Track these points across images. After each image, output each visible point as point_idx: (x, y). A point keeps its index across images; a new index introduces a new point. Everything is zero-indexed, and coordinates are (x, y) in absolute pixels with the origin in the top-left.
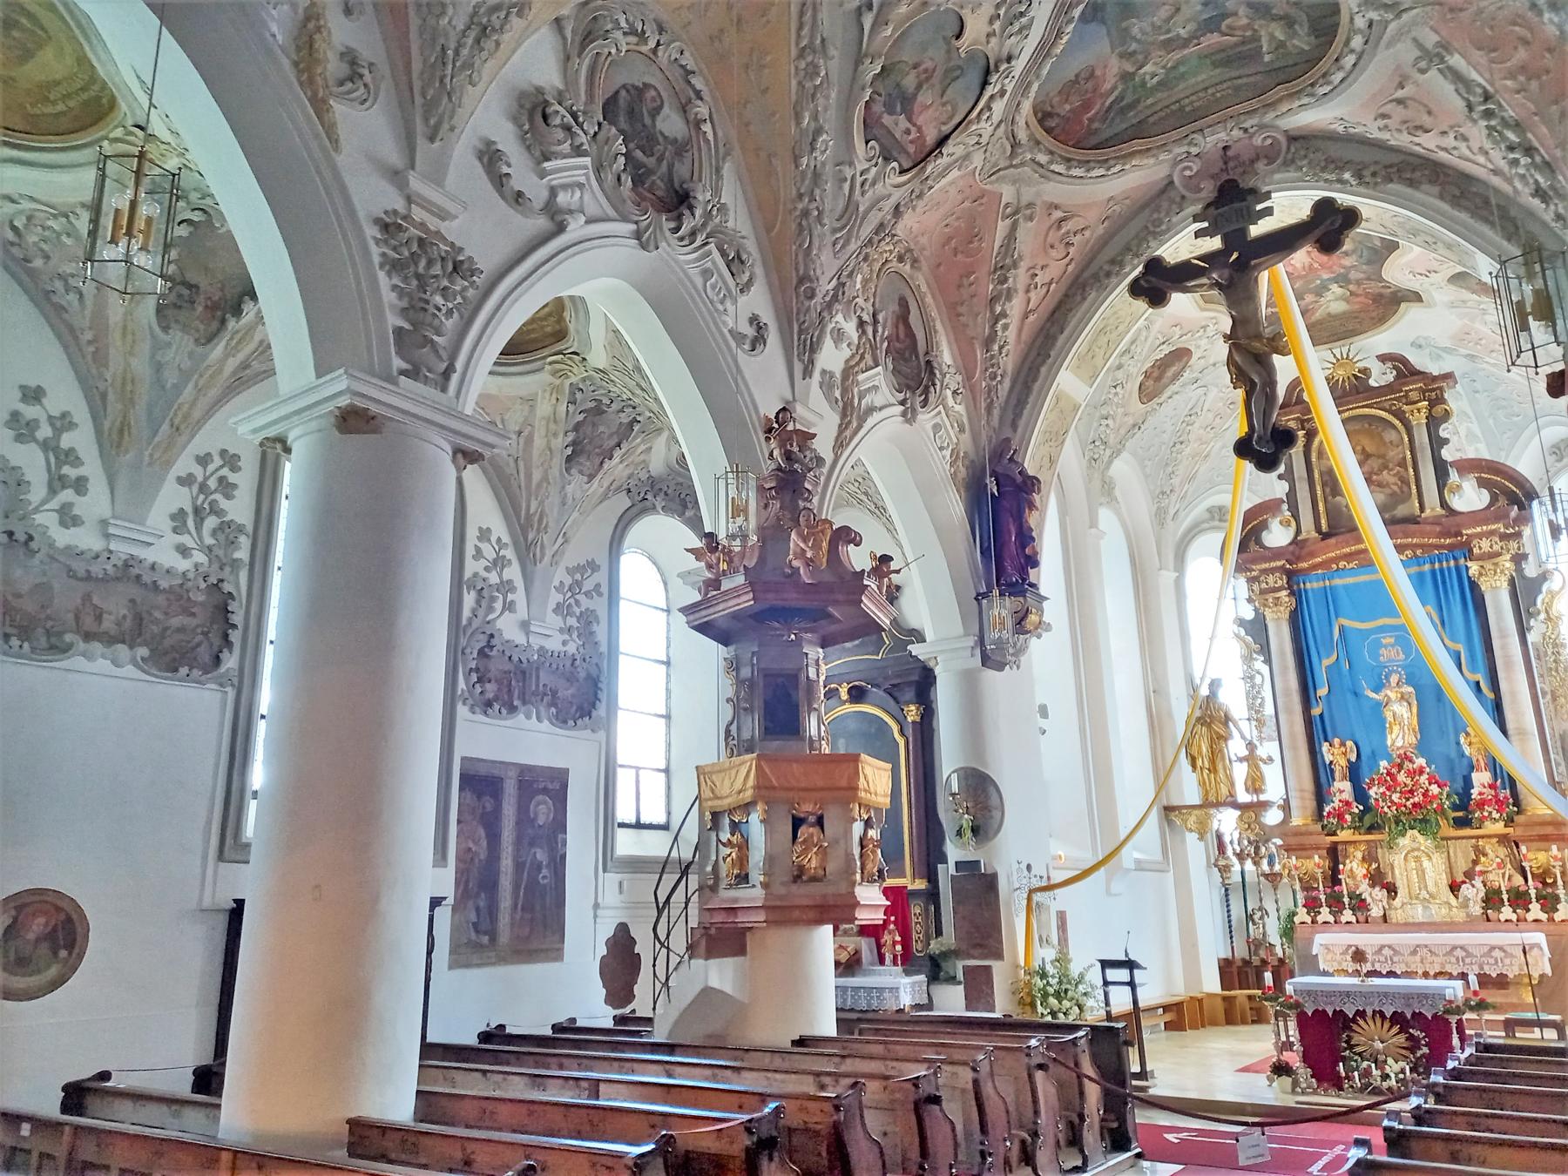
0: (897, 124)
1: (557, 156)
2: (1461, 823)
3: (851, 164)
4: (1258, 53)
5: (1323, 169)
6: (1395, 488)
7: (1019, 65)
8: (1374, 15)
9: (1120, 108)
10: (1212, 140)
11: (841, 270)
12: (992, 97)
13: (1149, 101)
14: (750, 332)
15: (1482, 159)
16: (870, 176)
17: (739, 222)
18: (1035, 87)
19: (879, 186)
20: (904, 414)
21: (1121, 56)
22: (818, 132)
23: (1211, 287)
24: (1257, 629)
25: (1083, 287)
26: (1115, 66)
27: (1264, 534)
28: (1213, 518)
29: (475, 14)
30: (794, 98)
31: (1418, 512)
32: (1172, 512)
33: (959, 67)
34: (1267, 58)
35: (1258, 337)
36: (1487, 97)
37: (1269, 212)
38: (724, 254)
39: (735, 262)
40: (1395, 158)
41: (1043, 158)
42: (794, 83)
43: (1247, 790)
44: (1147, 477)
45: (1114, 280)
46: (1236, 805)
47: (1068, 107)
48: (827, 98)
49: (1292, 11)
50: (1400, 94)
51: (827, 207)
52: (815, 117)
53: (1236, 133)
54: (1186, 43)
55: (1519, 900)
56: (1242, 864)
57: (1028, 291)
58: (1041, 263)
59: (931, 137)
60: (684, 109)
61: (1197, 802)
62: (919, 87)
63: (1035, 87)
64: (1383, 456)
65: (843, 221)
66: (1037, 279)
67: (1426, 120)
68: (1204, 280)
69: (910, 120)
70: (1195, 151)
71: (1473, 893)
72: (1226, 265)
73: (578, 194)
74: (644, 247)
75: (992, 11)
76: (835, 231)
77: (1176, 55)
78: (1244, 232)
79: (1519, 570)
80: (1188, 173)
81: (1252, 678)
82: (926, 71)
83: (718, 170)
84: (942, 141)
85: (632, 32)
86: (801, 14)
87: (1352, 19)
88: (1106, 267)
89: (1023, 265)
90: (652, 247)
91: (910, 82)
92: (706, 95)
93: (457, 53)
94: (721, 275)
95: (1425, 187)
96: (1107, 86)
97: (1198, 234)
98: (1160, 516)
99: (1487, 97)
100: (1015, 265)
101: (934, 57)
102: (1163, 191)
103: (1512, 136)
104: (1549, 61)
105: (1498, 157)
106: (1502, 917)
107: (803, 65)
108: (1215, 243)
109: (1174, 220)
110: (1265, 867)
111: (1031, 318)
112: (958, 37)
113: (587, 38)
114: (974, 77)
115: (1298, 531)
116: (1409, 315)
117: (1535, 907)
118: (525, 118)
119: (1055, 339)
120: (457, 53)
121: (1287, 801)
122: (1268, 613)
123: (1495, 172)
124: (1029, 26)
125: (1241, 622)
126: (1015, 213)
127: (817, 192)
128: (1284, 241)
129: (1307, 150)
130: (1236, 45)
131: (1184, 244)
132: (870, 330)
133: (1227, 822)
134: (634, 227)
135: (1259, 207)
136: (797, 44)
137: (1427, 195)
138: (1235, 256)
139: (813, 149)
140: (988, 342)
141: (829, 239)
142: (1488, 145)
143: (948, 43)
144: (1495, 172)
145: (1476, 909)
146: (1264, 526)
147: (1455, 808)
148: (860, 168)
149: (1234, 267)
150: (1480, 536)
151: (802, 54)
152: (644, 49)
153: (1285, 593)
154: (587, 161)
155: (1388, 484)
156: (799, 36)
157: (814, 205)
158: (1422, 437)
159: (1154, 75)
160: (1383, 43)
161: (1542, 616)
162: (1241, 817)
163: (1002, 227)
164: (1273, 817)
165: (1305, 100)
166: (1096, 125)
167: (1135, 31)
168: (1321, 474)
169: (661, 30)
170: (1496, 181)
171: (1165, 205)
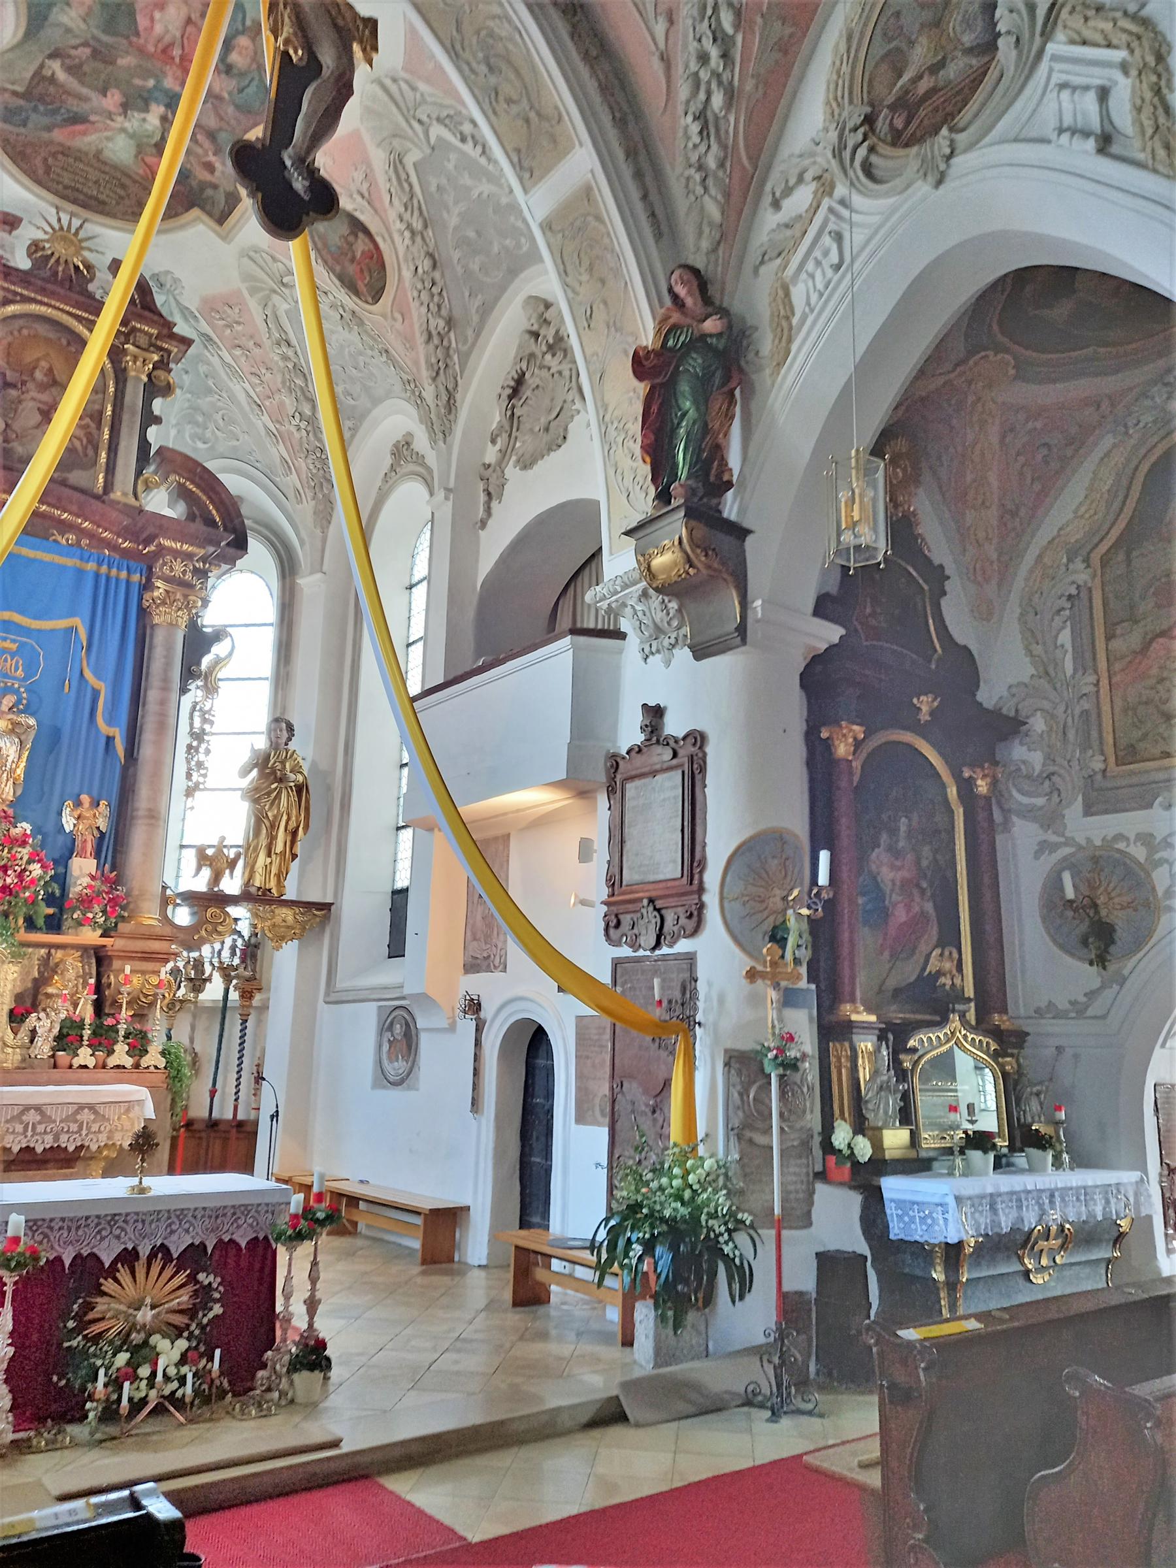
2: (53, 924)
55: (103, 1039)
71: (46, 1025)
106: (76, 1062)
117: (121, 1048)
145: (43, 1048)
147: (50, 900)
150: (176, 554)
158: (134, 395)
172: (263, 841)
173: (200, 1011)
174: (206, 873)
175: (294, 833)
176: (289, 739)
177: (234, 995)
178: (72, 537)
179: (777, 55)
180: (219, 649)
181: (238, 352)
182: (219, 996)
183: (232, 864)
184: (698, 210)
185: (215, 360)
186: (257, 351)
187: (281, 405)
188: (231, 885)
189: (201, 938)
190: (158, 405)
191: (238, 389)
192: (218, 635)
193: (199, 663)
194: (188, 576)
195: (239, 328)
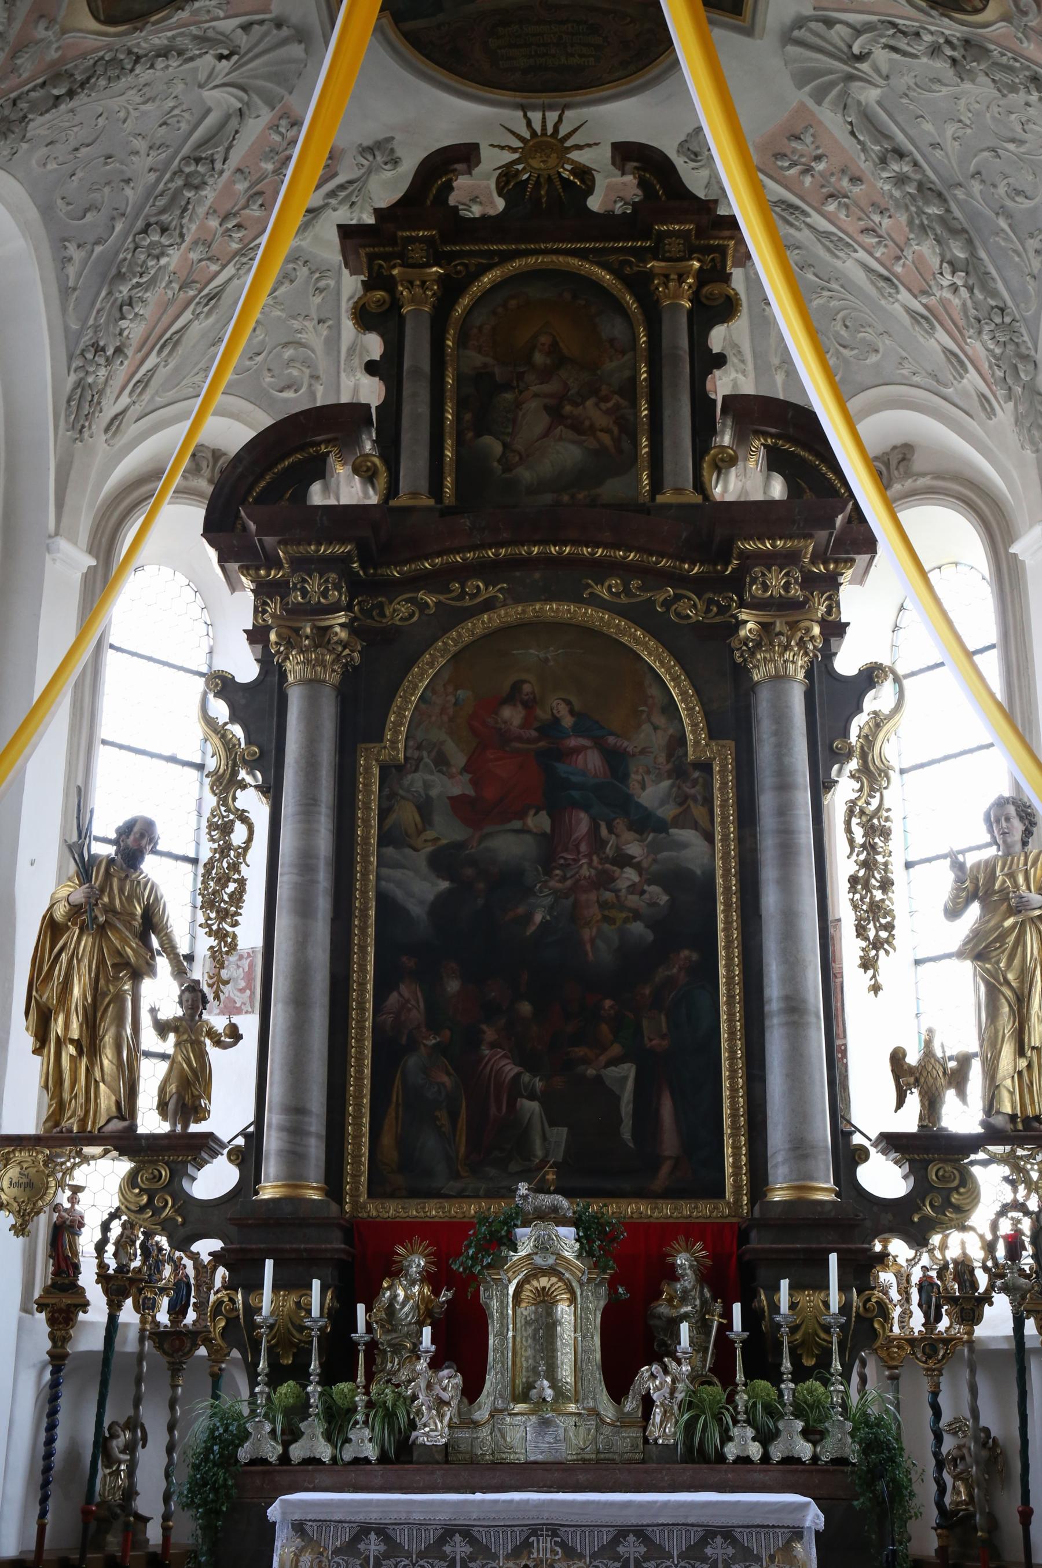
6: (606, 439)
24: (256, 706)
32: (110, 409)
43: (162, 1107)
44: (66, 291)
46: (126, 1142)
56: (115, 1306)
79: (829, 655)
81: (226, 829)
98: (80, 406)
110: (163, 1317)
121: (254, 1138)
122: (294, 667)
125: (223, 685)
133: (100, 1185)
150: (768, 560)
153: (342, 618)
155: (592, 430)
161: (853, 764)
162: (131, 1180)
164: (213, 1180)
168: (459, 379)
172: (1006, 1024)
173: (980, 1357)
174: (913, 1100)
176: (1028, 833)
181: (831, 207)
182: (1007, 1329)
183: (958, 1079)
185: (804, 236)
186: (857, 190)
187: (919, 263)
188: (962, 1116)
189: (925, 1218)
190: (718, 338)
192: (870, 676)
193: (845, 733)
194: (796, 591)
195: (820, 167)
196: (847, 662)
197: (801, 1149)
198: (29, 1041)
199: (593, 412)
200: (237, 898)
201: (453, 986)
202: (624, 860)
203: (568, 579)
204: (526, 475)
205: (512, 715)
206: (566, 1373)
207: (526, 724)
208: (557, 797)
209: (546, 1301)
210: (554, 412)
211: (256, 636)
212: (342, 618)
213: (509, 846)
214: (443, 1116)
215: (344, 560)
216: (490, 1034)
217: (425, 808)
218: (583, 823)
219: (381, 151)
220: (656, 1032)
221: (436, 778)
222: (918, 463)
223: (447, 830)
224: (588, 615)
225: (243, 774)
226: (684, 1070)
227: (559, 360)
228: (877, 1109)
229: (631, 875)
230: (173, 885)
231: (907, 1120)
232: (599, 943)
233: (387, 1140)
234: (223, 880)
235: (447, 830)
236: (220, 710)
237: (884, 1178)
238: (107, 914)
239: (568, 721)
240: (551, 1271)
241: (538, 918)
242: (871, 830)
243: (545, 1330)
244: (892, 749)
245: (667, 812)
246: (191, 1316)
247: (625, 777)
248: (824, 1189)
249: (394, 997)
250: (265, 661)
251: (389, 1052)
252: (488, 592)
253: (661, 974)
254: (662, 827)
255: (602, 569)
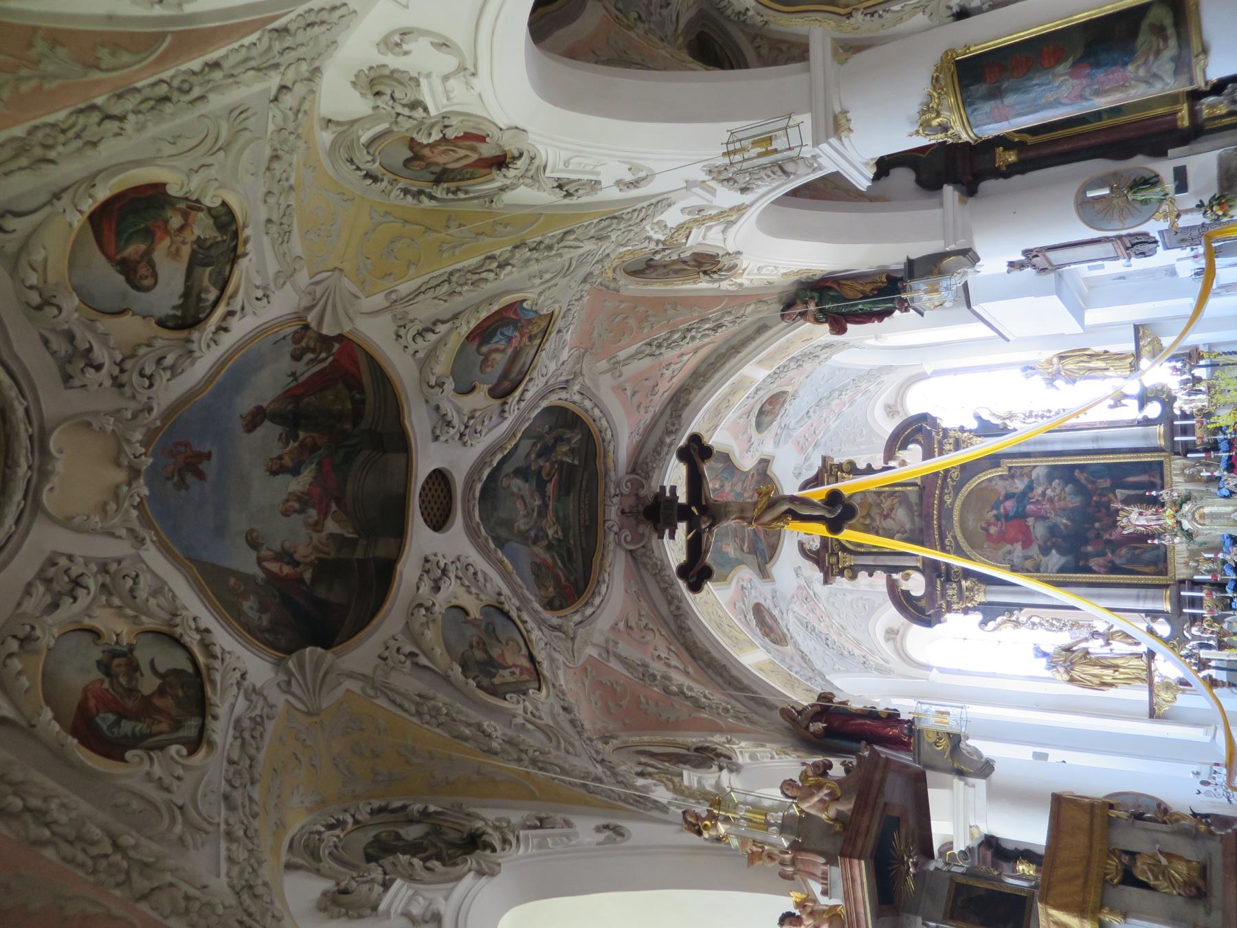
0: (505, 676)
1: (380, 899)
3: (514, 716)
4: (571, 466)
5: (659, 454)
7: (506, 590)
8: (577, 388)
9: (568, 559)
10: (612, 513)
11: (591, 757)
12: (519, 617)
13: (572, 542)
14: (607, 833)
15: (685, 358)
16: (530, 708)
17: (516, 817)
18: (527, 593)
19: (540, 706)
20: (731, 771)
21: (534, 543)
22: (479, 726)
23: (710, 532)
25: (681, 628)
26: (539, 550)
27: (913, 593)
28: (894, 639)
29: (232, 887)
30: (447, 735)
31: (916, 488)
33: (488, 624)
34: (576, 462)
35: (755, 504)
36: (650, 344)
37: (673, 489)
38: (535, 827)
39: (542, 823)
40: (668, 412)
41: (577, 618)
42: (437, 730)
44: (848, 671)
45: (683, 605)
47: (551, 589)
48: (459, 712)
49: (554, 434)
50: (629, 392)
51: (537, 744)
52: (469, 725)
53: (616, 500)
54: (545, 506)
56: (1210, 667)
57: (669, 666)
58: (652, 649)
59: (525, 663)
60: (410, 821)
61: (1147, 693)
62: (486, 652)
63: (527, 593)
64: (871, 505)
65: (554, 739)
66: (663, 656)
67: (649, 384)
68: (705, 535)
69: (505, 668)
70: (616, 529)
72: (698, 518)
73: (420, 899)
74: (493, 875)
75: (463, 589)
76: (558, 747)
77: (550, 513)
78: (681, 506)
79: (970, 431)
80: (629, 539)
81: (1034, 624)
82: (478, 643)
83: (468, 814)
84: (532, 658)
85: (331, 827)
86: (393, 702)
87: (574, 403)
88: (673, 608)
89: (648, 660)
90: (497, 868)
91: (479, 655)
92: (407, 803)
93: (250, 915)
94: (549, 835)
95: (691, 396)
96: (550, 561)
97: (672, 536)
98: (882, 670)
99: (650, 344)
100: (645, 666)
101: (471, 633)
102: (634, 559)
103: (676, 336)
104: (641, 309)
105: (688, 346)
107: (427, 717)
108: (682, 527)
109: (657, 554)
111: (690, 670)
112: (467, 613)
113: (315, 855)
114: (499, 620)
115: (915, 568)
116: (776, 470)
118: (336, 910)
119: (712, 658)
120: (250, 915)
122: (981, 598)
123: (696, 351)
124: (485, 575)
125: (984, 623)
126: (608, 652)
127: (522, 747)
128: (695, 481)
129: (643, 465)
130: (560, 476)
131: (674, 549)
132: (650, 770)
134: (472, 874)
135: (668, 494)
136: (412, 715)
137: (696, 397)
138: (694, 509)
139: (489, 736)
140: (701, 707)
141: (562, 754)
142: (677, 351)
143: (466, 622)
144: (696, 351)
146: (906, 593)
148: (521, 711)
149: (700, 511)
151: (419, 714)
152: (350, 826)
153: (963, 583)
154: (398, 882)
156: (406, 711)
157: (531, 751)
159: (556, 532)
160: (593, 390)
161: (1007, 422)
163: (614, 664)
165: (611, 448)
166: (572, 578)
167: (523, 527)
169: (345, 811)
170: (702, 354)
171: (646, 560)
172: (1100, 373)
174: (1124, 402)
175: (1091, 356)
177: (1202, 362)
178: (946, 497)
179: (679, 307)
180: (986, 416)
182: (1204, 369)
184: (751, 315)
191: (833, 425)
192: (978, 418)
194: (951, 441)
196: (973, 425)
197: (1146, 437)
198: (1112, 690)
199: (886, 504)
200: (1059, 620)
201: (1090, 548)
202: (1044, 494)
203: (945, 513)
204: (908, 526)
205: (993, 530)
206: (1230, 509)
207: (995, 525)
208: (1021, 515)
209: (1203, 516)
210: (886, 517)
211: (966, 611)
212: (963, 583)
213: (1039, 530)
214: (1137, 552)
215: (942, 583)
216: (1107, 536)
217: (1026, 558)
218: (1030, 507)
219: (798, 572)
220: (1105, 483)
221: (1015, 554)
222: (891, 402)
223: (1034, 550)
224: (958, 503)
225: (1014, 618)
226: (1118, 474)
227: (868, 515)
228: (1130, 411)
229: (1049, 492)
230: (1055, 640)
231: (1135, 403)
232: (1075, 501)
233: (1146, 570)
234: (1052, 625)
235: (1034, 550)
236: (992, 624)
237: (1154, 410)
238: (1069, 660)
239: (995, 512)
240: (1193, 514)
241: (1064, 521)
242: (1030, 416)
243: (1213, 516)
244: (1002, 411)
245: (1026, 480)
246: (1212, 642)
247: (1014, 494)
248: (1160, 429)
249: (1095, 568)
250: (975, 609)
251: (1114, 569)
252: (950, 538)
253: (1083, 481)
254: (1032, 482)
255: (942, 502)
